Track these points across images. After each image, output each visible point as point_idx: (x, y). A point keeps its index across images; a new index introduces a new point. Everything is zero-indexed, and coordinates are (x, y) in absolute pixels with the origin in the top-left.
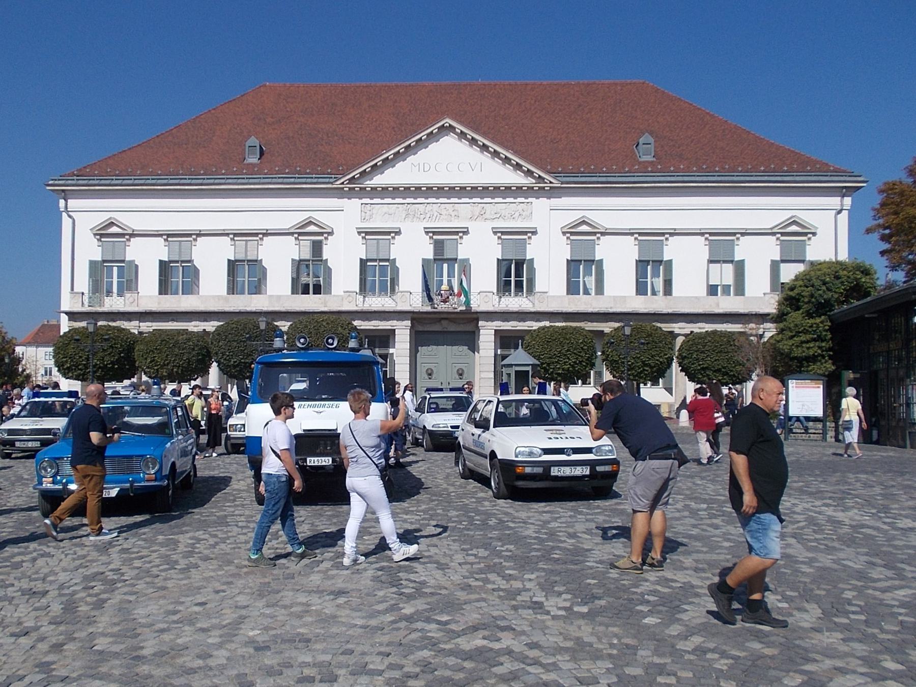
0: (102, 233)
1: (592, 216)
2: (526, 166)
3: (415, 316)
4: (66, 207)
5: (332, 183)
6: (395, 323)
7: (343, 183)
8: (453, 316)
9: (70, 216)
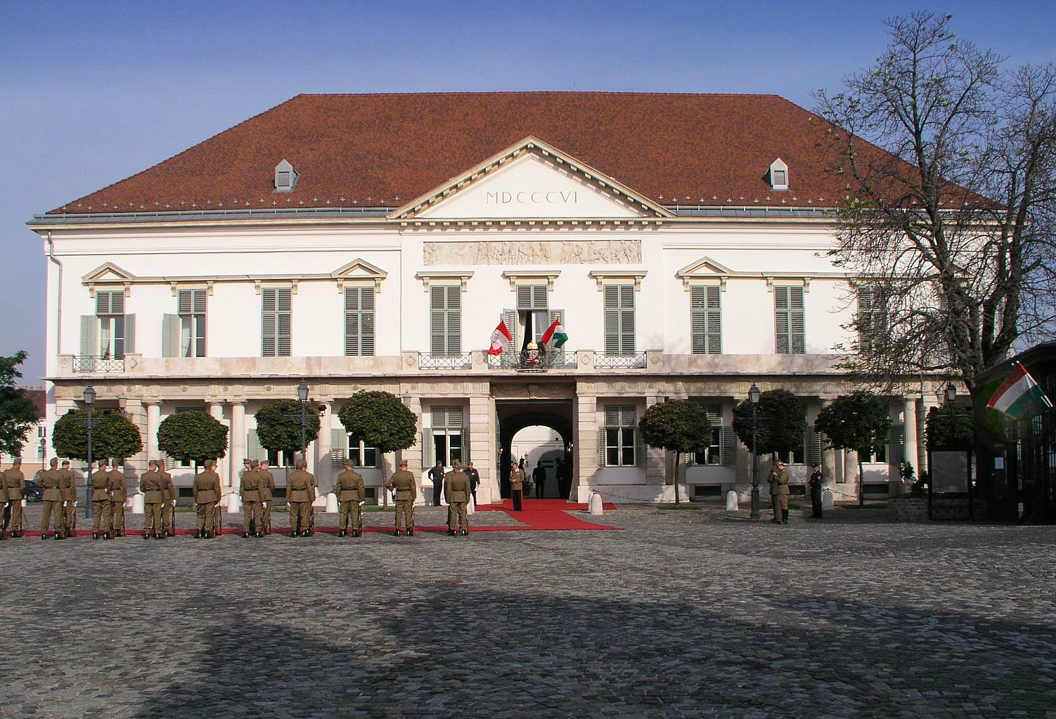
2: (632, 196)
3: (495, 381)
4: (52, 251)
7: (400, 217)
9: (57, 262)
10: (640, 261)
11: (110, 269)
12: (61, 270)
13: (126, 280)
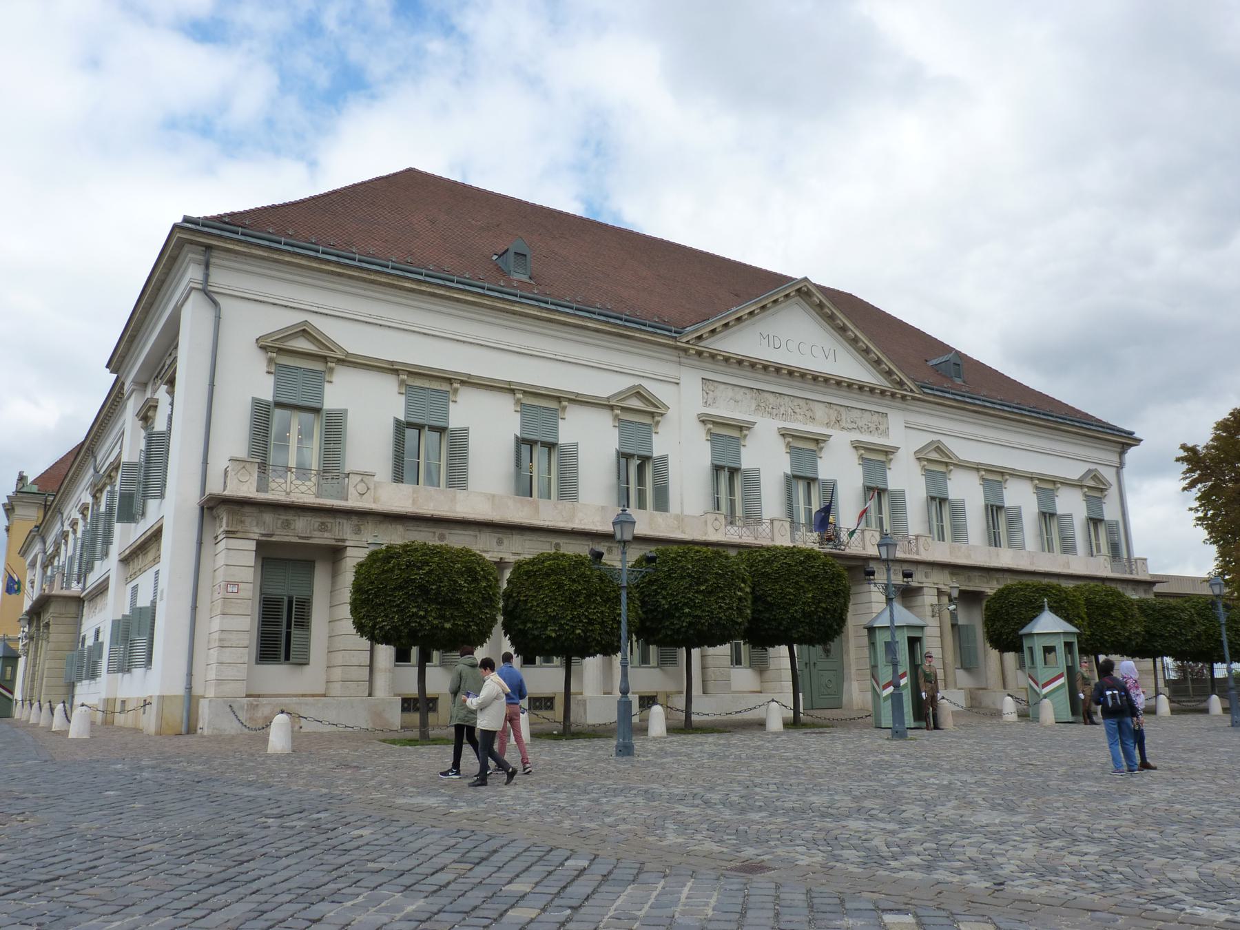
0: (274, 348)
1: (950, 443)
2: (888, 364)
7: (688, 342)
11: (304, 332)
12: (218, 318)
13: (330, 359)
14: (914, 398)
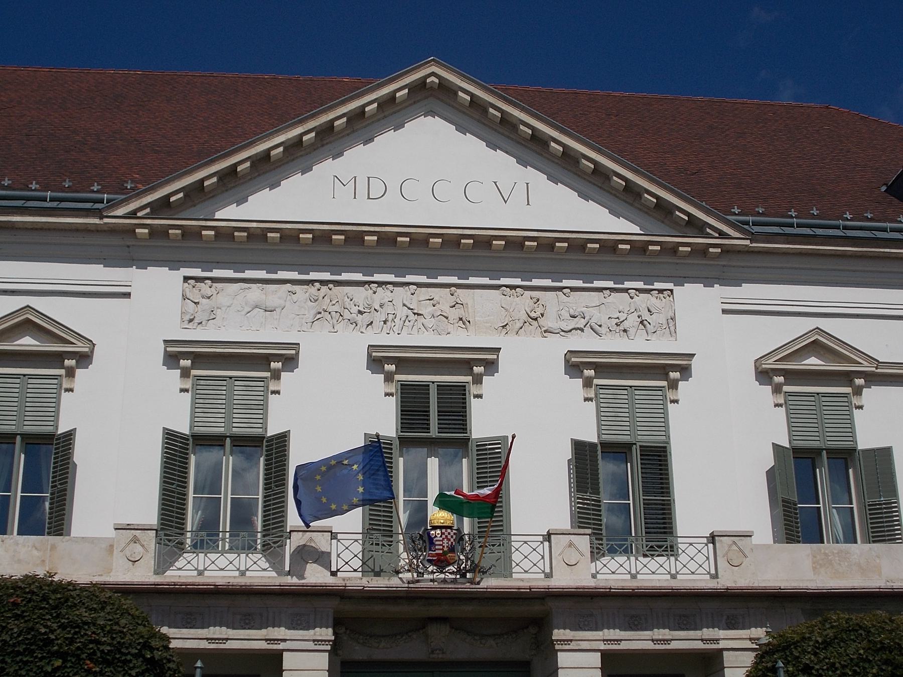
5: (99, 214)
6: (280, 632)
7: (133, 214)
8: (468, 609)
10: (673, 333)
14: (727, 251)
